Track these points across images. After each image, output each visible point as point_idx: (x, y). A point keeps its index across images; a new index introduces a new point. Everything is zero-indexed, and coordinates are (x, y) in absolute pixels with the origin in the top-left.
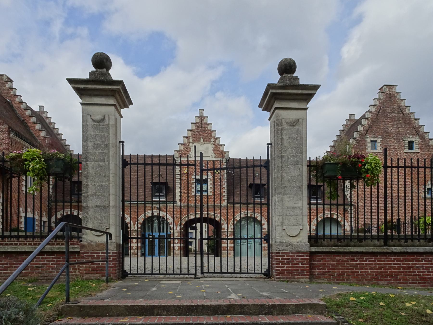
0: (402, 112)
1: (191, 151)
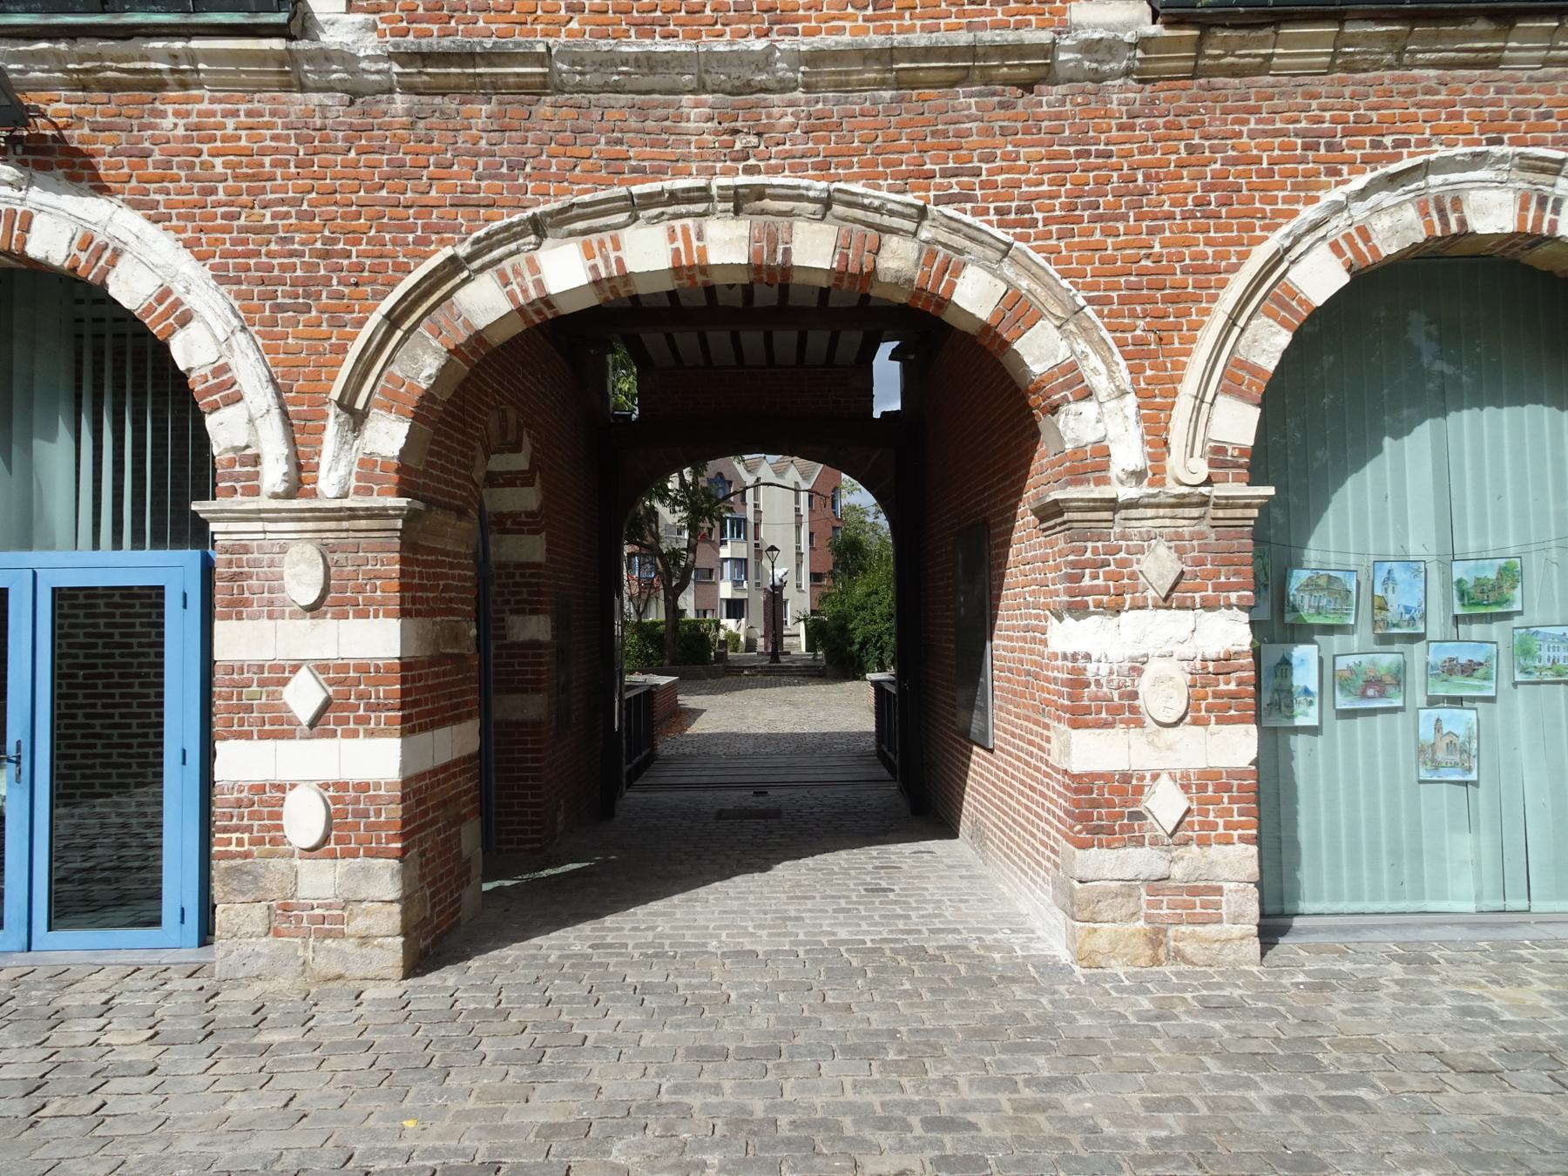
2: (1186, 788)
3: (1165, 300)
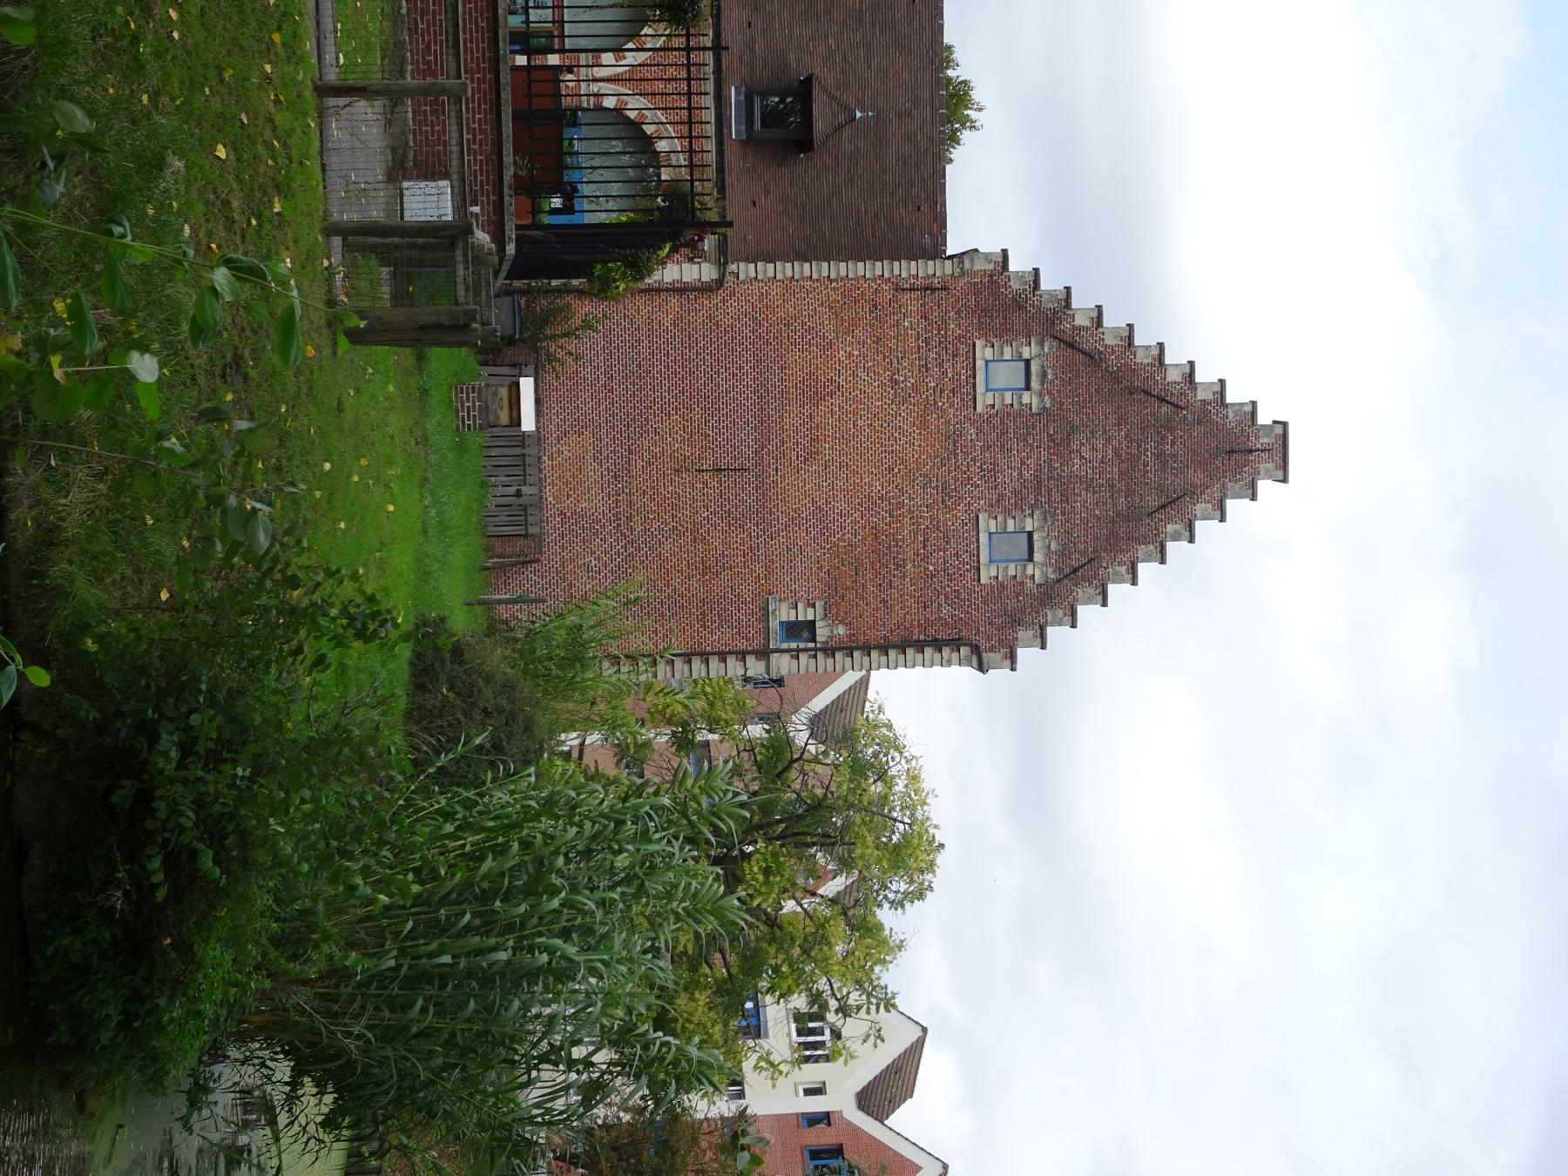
0: (1163, 507)
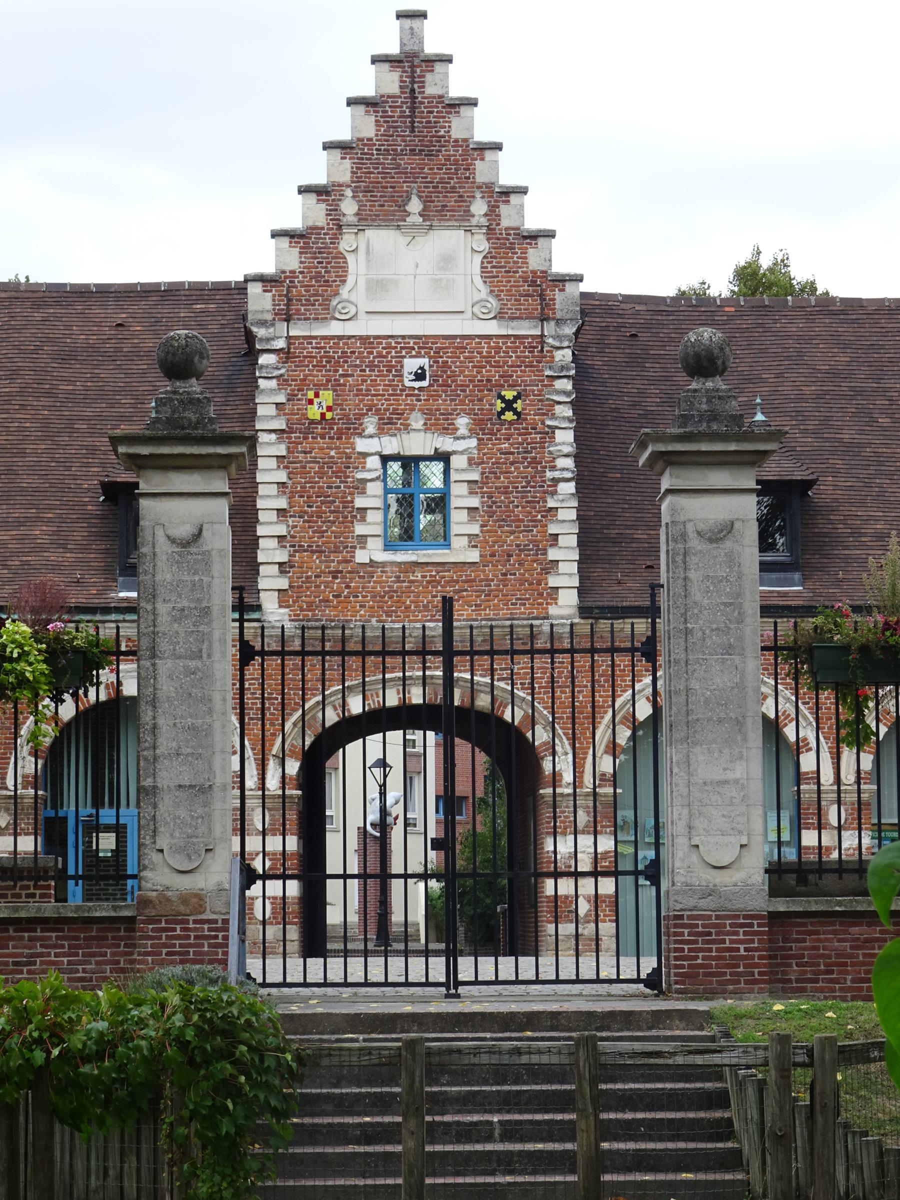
1: (351, 280)
2: (589, 901)
3: (584, 718)
